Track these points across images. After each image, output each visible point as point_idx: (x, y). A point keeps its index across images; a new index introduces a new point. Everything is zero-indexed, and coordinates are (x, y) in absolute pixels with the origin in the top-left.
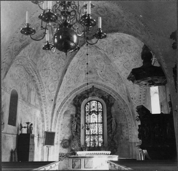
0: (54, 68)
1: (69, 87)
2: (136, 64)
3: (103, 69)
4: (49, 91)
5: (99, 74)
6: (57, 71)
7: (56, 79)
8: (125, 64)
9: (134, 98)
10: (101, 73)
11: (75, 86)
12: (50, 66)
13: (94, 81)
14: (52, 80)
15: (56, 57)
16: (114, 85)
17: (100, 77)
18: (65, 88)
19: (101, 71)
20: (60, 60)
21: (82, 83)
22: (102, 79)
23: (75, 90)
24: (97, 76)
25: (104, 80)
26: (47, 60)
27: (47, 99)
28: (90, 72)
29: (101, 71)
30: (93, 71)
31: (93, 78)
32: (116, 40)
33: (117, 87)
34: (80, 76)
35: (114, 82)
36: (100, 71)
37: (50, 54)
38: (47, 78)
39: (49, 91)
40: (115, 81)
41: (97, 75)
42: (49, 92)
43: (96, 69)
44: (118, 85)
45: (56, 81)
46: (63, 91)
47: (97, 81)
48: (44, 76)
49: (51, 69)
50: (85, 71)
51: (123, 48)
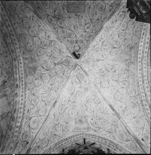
0: (44, 99)
1: (55, 135)
2: (127, 90)
3: (93, 116)
4: (29, 126)
5: (89, 123)
6: (46, 104)
7: (42, 114)
8: (115, 96)
9: (145, 137)
10: (91, 121)
11: (63, 136)
12: (40, 96)
13: (85, 132)
14: (37, 113)
15: (48, 89)
16: (110, 132)
17: (92, 127)
18: (50, 133)
19: (92, 119)
20: (51, 92)
21: (72, 133)
22: (94, 128)
23: (62, 141)
24: (88, 126)
25: (97, 129)
26: (40, 87)
27: (21, 135)
28: (80, 121)
29: (92, 119)
30: (84, 120)
31: (84, 129)
32: (102, 69)
33: (114, 134)
34: (69, 123)
35: (109, 127)
36: (91, 119)
37: (44, 82)
38: (32, 106)
39: (29, 126)
40: (109, 125)
41: (88, 124)
42: (28, 128)
43: (87, 118)
44: (115, 130)
45: (42, 117)
46: (47, 137)
47: (89, 132)
48: (30, 101)
49: (40, 99)
50: (75, 119)
51: (110, 78)
